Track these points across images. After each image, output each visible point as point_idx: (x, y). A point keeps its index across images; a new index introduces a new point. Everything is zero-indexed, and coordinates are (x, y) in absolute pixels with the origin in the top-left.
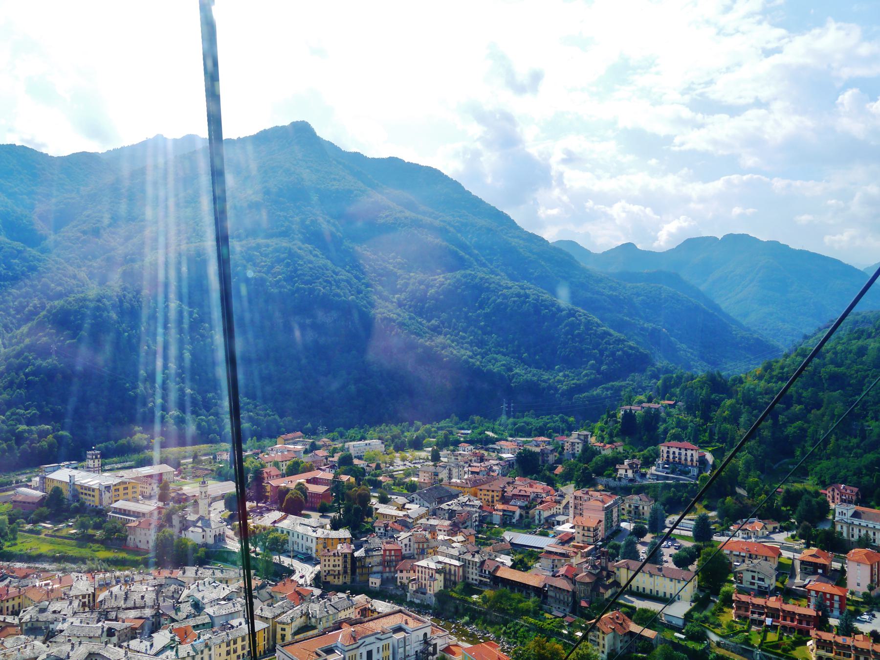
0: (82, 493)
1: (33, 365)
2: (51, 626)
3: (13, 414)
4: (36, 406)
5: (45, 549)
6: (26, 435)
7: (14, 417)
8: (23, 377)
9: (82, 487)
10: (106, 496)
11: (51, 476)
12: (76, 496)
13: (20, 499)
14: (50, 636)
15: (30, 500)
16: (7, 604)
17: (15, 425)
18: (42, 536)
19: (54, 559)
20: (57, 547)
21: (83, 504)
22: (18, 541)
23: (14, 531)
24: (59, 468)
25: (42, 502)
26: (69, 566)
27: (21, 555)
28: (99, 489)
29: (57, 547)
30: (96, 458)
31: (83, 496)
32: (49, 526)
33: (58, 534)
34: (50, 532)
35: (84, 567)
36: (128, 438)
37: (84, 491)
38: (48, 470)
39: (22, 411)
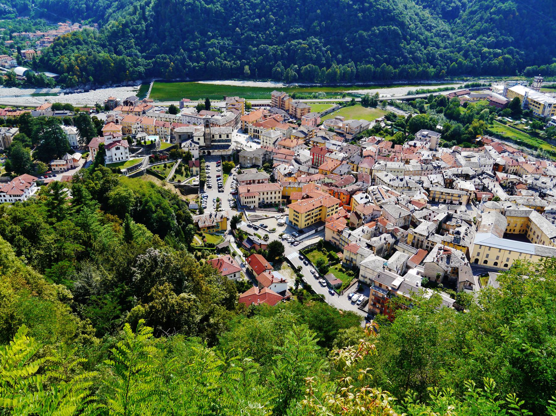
0: (531, 104)
1: (496, 7)
2: (542, 190)
3: (481, 40)
4: (494, 36)
5: (509, 134)
6: (487, 55)
7: (482, 42)
8: (489, 15)
9: (532, 101)
10: (547, 110)
11: (512, 89)
12: (527, 105)
13: (494, 100)
14: (543, 196)
15: (501, 102)
16: (511, 168)
17: (481, 47)
18: (507, 125)
19: (516, 143)
20: (517, 136)
21: (532, 111)
22: (494, 125)
23: (492, 119)
24: (517, 84)
25: (507, 105)
26: (525, 149)
27: (497, 135)
28: (544, 105)
29: (517, 136)
30: (540, 82)
31: (532, 106)
32: (511, 120)
33: (516, 127)
34: (512, 124)
35: (535, 153)
36: (547, 65)
37: (533, 103)
38: (510, 84)
39: (486, 38)
